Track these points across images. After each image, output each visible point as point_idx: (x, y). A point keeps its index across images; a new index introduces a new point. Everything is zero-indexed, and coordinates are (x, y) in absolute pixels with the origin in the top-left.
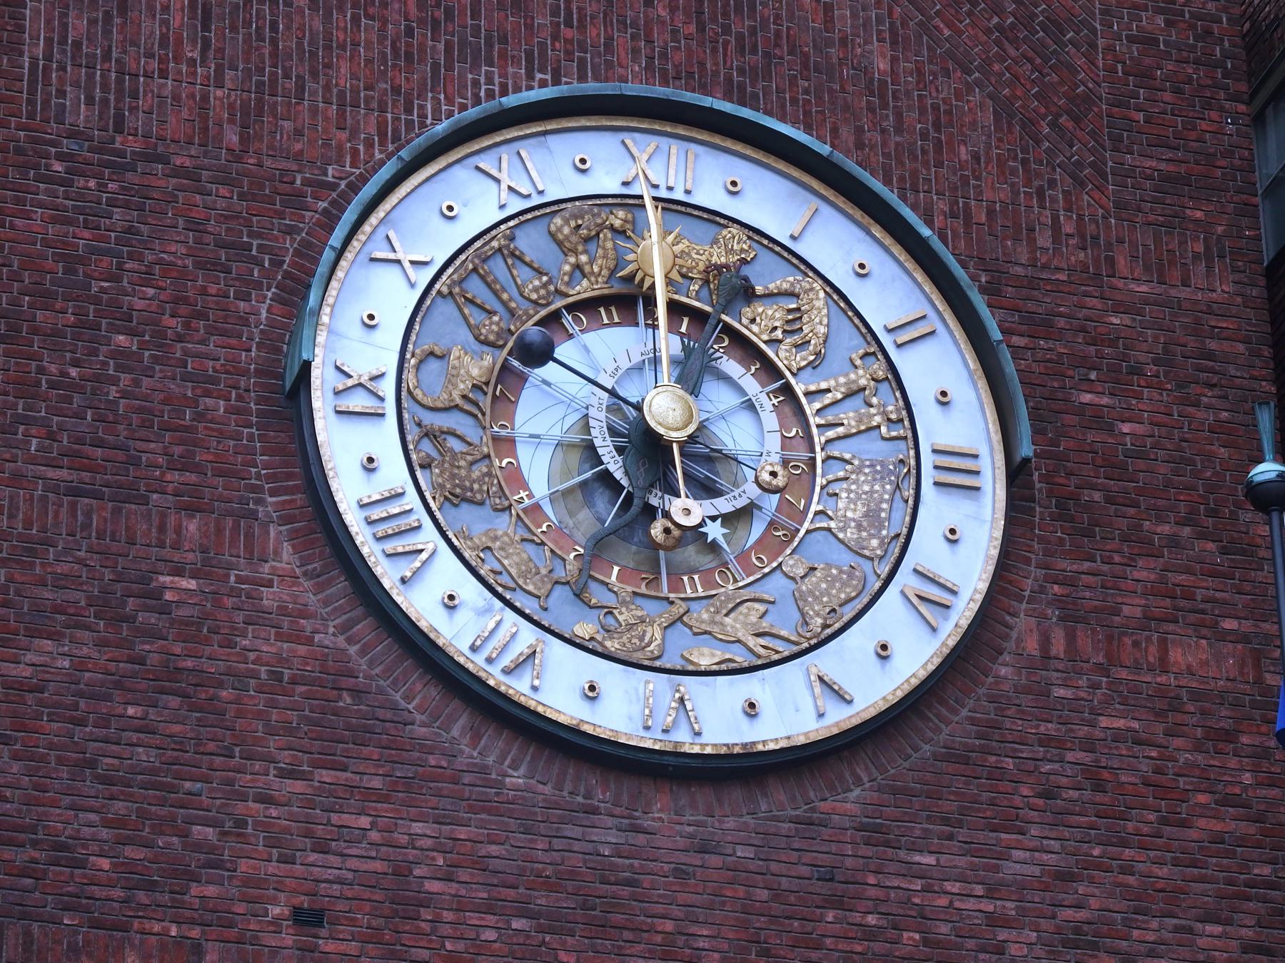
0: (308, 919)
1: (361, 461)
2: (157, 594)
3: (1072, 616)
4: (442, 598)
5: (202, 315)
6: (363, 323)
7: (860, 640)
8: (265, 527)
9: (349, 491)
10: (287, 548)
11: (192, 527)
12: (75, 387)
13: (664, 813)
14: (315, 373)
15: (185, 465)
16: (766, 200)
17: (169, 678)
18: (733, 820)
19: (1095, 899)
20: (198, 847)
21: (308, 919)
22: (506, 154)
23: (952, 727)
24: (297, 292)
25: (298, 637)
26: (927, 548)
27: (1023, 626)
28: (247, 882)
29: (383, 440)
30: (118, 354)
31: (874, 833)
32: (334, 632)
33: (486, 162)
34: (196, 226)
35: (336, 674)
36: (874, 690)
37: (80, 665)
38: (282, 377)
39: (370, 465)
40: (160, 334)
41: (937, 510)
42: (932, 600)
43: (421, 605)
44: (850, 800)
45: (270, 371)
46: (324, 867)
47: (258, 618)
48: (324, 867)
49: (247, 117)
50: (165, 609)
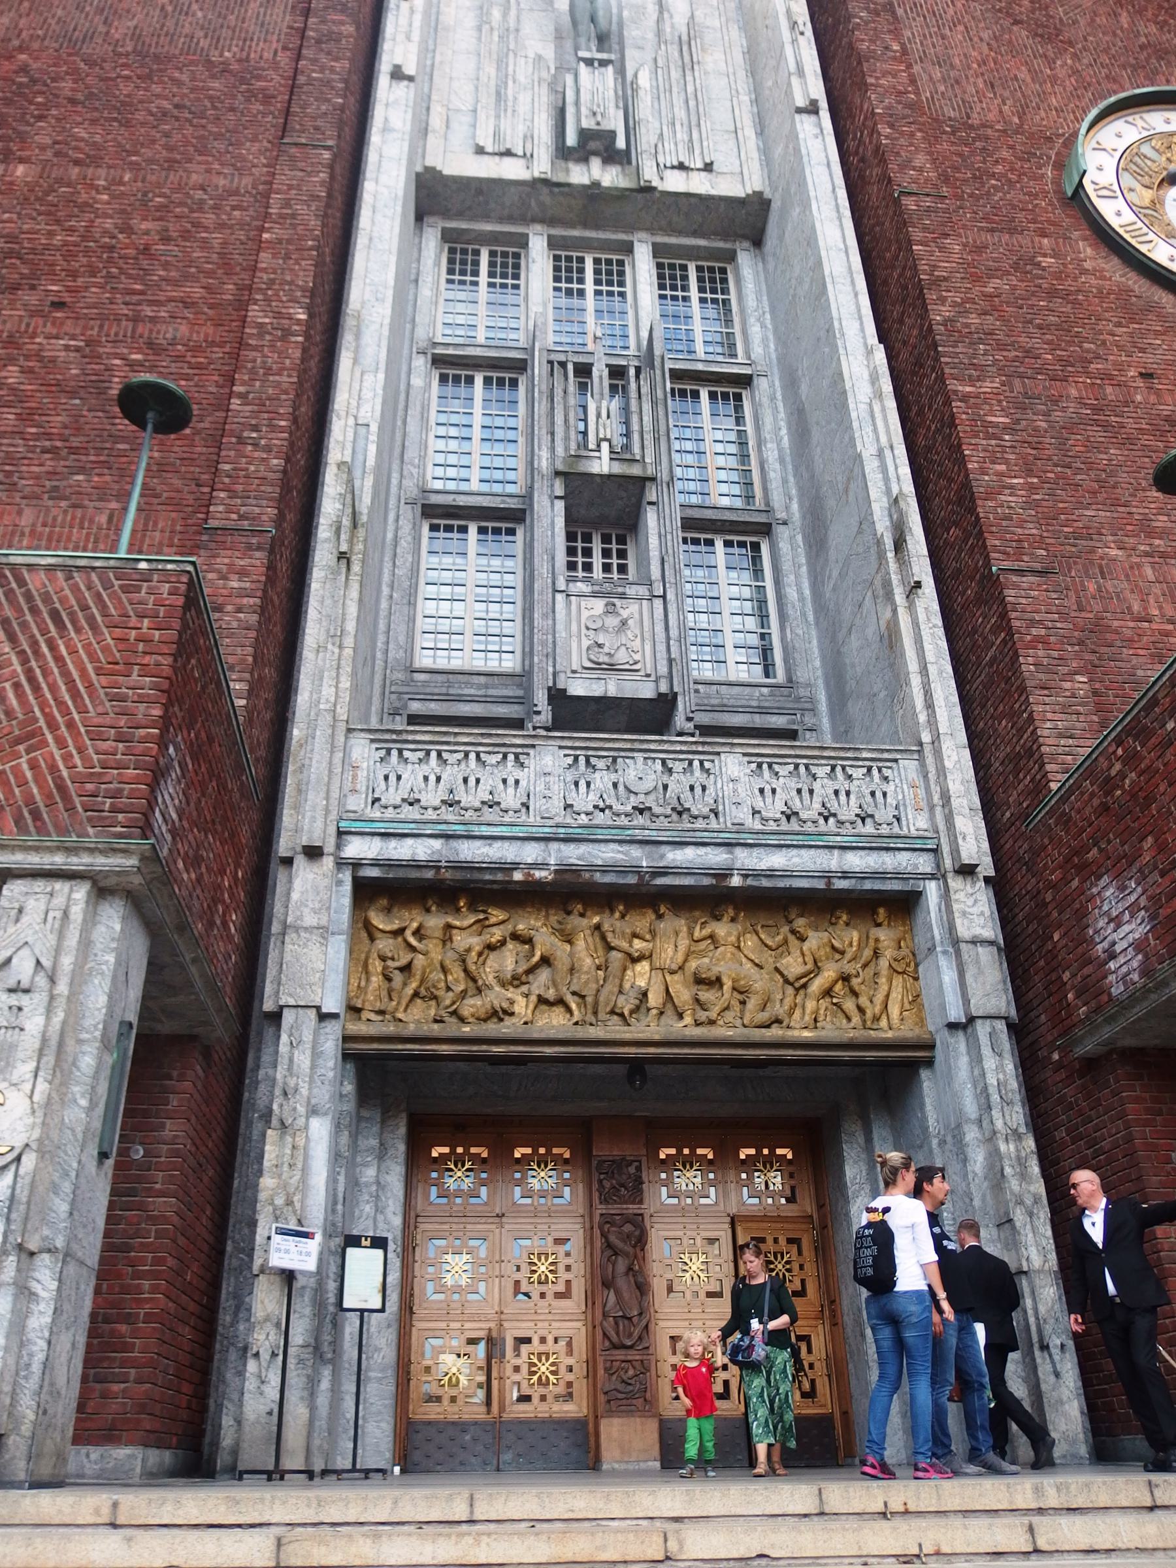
0: (1146, 376)
1: (1116, 213)
2: (1039, 264)
5: (1024, 174)
8: (1077, 241)
9: (1115, 222)
10: (1089, 250)
11: (1046, 241)
12: (978, 198)
14: (1086, 182)
15: (1034, 221)
17: (1052, 294)
20: (1088, 351)
22: (1137, 116)
25: (1103, 278)
28: (1115, 363)
29: (1120, 204)
30: (993, 186)
33: (1130, 119)
34: (1012, 147)
35: (1124, 292)
37: (1014, 288)
38: (1065, 193)
39: (1119, 214)
40: (1010, 180)
45: (1060, 191)
46: (1149, 358)
47: (1085, 272)
48: (1149, 358)
50: (1044, 269)
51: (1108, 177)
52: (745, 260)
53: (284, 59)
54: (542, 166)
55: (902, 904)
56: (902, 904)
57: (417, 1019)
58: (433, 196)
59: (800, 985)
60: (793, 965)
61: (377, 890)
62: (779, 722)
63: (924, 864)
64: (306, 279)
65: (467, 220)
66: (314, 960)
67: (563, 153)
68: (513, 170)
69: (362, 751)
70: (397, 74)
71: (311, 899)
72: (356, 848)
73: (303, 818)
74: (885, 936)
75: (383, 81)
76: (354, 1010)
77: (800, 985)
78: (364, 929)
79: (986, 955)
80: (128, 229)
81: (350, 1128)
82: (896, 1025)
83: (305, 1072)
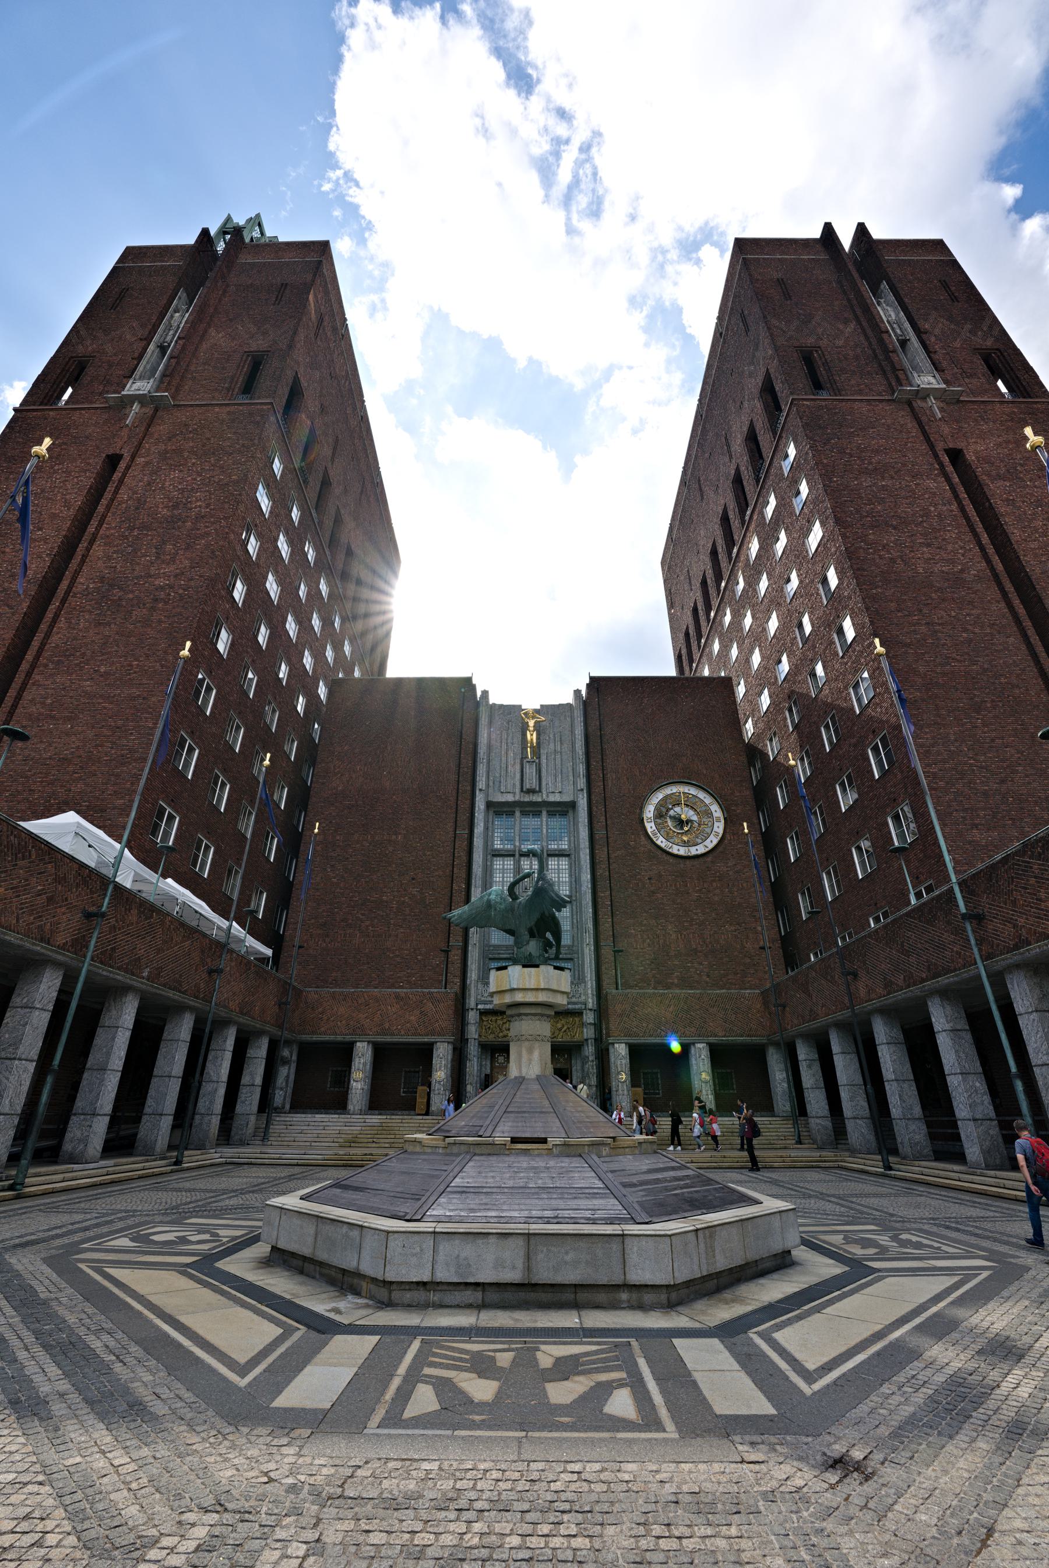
0: (650, 879)
1: (650, 827)
3: (734, 835)
4: (661, 841)
6: (649, 811)
7: (708, 840)
9: (649, 831)
13: (687, 862)
16: (693, 791)
18: (696, 862)
19: (739, 867)
21: (650, 879)
23: (720, 849)
24: (641, 809)
26: (715, 829)
27: (728, 836)
31: (712, 862)
32: (649, 846)
35: (650, 851)
36: (711, 846)
41: (716, 824)
42: (717, 834)
43: (658, 842)
44: (709, 858)
49: (634, 790)
51: (651, 815)
52: (571, 814)
53: (454, 794)
54: (517, 798)
55: (579, 1014)
56: (579, 1014)
57: (491, 1037)
58: (489, 805)
59: (560, 1030)
60: (559, 1026)
61: (483, 1013)
62: (569, 956)
63: (583, 1007)
64: (464, 876)
65: (498, 809)
66: (472, 1032)
67: (522, 790)
68: (510, 798)
69: (480, 986)
70: (480, 790)
71: (472, 1016)
72: (479, 1007)
73: (471, 1002)
74: (577, 1019)
75: (477, 792)
76: (480, 1036)
77: (560, 1030)
78: (481, 1019)
79: (592, 1027)
80: (425, 855)
81: (480, 1058)
82: (577, 1038)
83: (473, 1049)
